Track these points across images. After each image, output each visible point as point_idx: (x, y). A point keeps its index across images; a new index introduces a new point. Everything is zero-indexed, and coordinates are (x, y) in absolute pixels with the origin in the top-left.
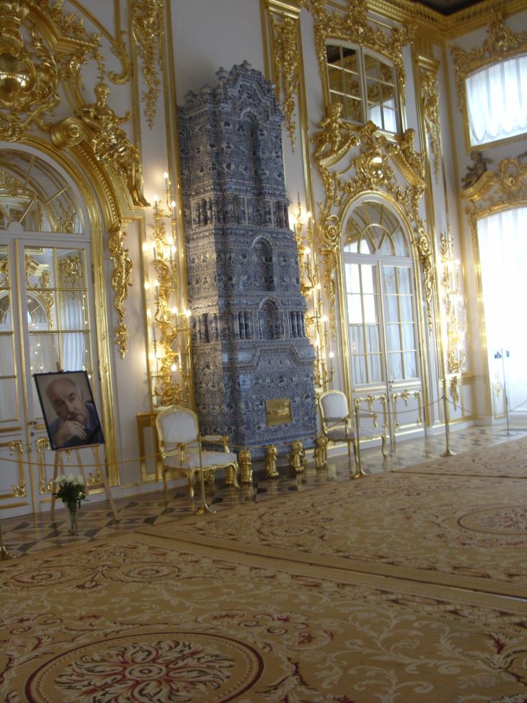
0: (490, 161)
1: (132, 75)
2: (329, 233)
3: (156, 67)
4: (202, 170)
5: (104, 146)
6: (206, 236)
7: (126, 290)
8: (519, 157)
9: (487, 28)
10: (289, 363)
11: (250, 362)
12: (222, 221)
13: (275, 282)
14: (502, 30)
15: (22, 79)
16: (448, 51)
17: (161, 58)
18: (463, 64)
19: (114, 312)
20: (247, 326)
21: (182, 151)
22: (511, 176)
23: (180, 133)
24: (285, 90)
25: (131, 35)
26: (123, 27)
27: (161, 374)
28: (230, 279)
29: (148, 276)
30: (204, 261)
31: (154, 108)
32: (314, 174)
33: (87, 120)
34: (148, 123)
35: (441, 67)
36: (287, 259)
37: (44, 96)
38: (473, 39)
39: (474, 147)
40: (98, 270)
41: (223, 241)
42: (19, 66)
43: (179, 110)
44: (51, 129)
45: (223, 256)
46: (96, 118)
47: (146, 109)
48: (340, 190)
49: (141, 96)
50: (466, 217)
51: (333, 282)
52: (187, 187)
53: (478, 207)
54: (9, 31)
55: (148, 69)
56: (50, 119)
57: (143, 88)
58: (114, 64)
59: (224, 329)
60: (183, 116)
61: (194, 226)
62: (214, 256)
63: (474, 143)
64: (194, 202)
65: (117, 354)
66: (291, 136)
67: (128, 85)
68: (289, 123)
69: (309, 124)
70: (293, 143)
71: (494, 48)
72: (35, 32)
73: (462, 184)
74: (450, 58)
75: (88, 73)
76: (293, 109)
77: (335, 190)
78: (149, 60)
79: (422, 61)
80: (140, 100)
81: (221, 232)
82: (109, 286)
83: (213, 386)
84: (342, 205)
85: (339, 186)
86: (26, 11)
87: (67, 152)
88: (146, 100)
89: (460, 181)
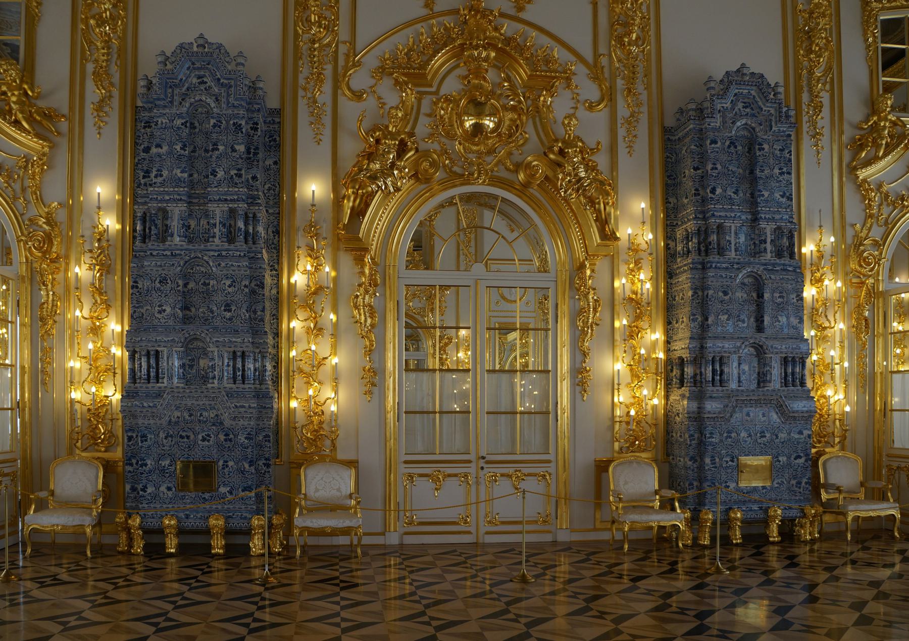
1: (611, 100)
2: (864, 260)
3: (640, 87)
4: (686, 198)
5: (570, 181)
6: (686, 271)
7: (592, 330)
10: (775, 416)
11: (720, 413)
12: (703, 254)
13: (766, 323)
15: (490, 120)
17: (646, 76)
19: (577, 352)
20: (722, 372)
21: (668, 177)
23: (668, 157)
24: (810, 91)
25: (610, 55)
26: (602, 50)
27: (625, 419)
28: (707, 319)
29: (619, 315)
30: (682, 299)
31: (634, 133)
32: (849, 189)
33: (552, 156)
34: (628, 150)
36: (784, 294)
37: (510, 136)
40: (564, 309)
41: (701, 276)
42: (487, 110)
43: (667, 131)
44: (518, 166)
45: (700, 293)
46: (561, 152)
47: (625, 134)
48: (888, 205)
49: (619, 121)
51: (866, 320)
52: (672, 216)
54: (477, 77)
55: (629, 91)
56: (517, 158)
57: (623, 111)
58: (591, 91)
59: (695, 375)
60: (671, 138)
61: (679, 260)
62: (690, 293)
64: (679, 233)
65: (578, 396)
66: (817, 145)
67: (606, 109)
68: (815, 129)
69: (846, 127)
70: (818, 153)
72: (504, 72)
75: (558, 105)
76: (820, 111)
77: (880, 205)
78: (631, 80)
80: (619, 125)
81: (700, 266)
82: (573, 324)
83: (681, 436)
84: (889, 225)
85: (886, 199)
86: (493, 54)
87: (534, 191)
88: (626, 125)
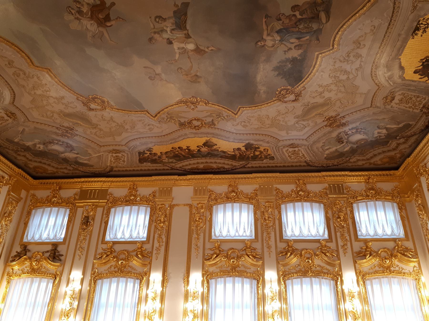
0: (29, 251)
8: (43, 252)
9: (51, 191)
14: (56, 193)
16: (30, 195)
18: (34, 203)
22: (36, 261)
35: (22, 202)
38: (42, 194)
39: (24, 242)
50: (6, 277)
53: (15, 273)
63: (25, 240)
71: (51, 200)
73: (11, 259)
74: (29, 199)
79: (12, 195)
89: (11, 257)
